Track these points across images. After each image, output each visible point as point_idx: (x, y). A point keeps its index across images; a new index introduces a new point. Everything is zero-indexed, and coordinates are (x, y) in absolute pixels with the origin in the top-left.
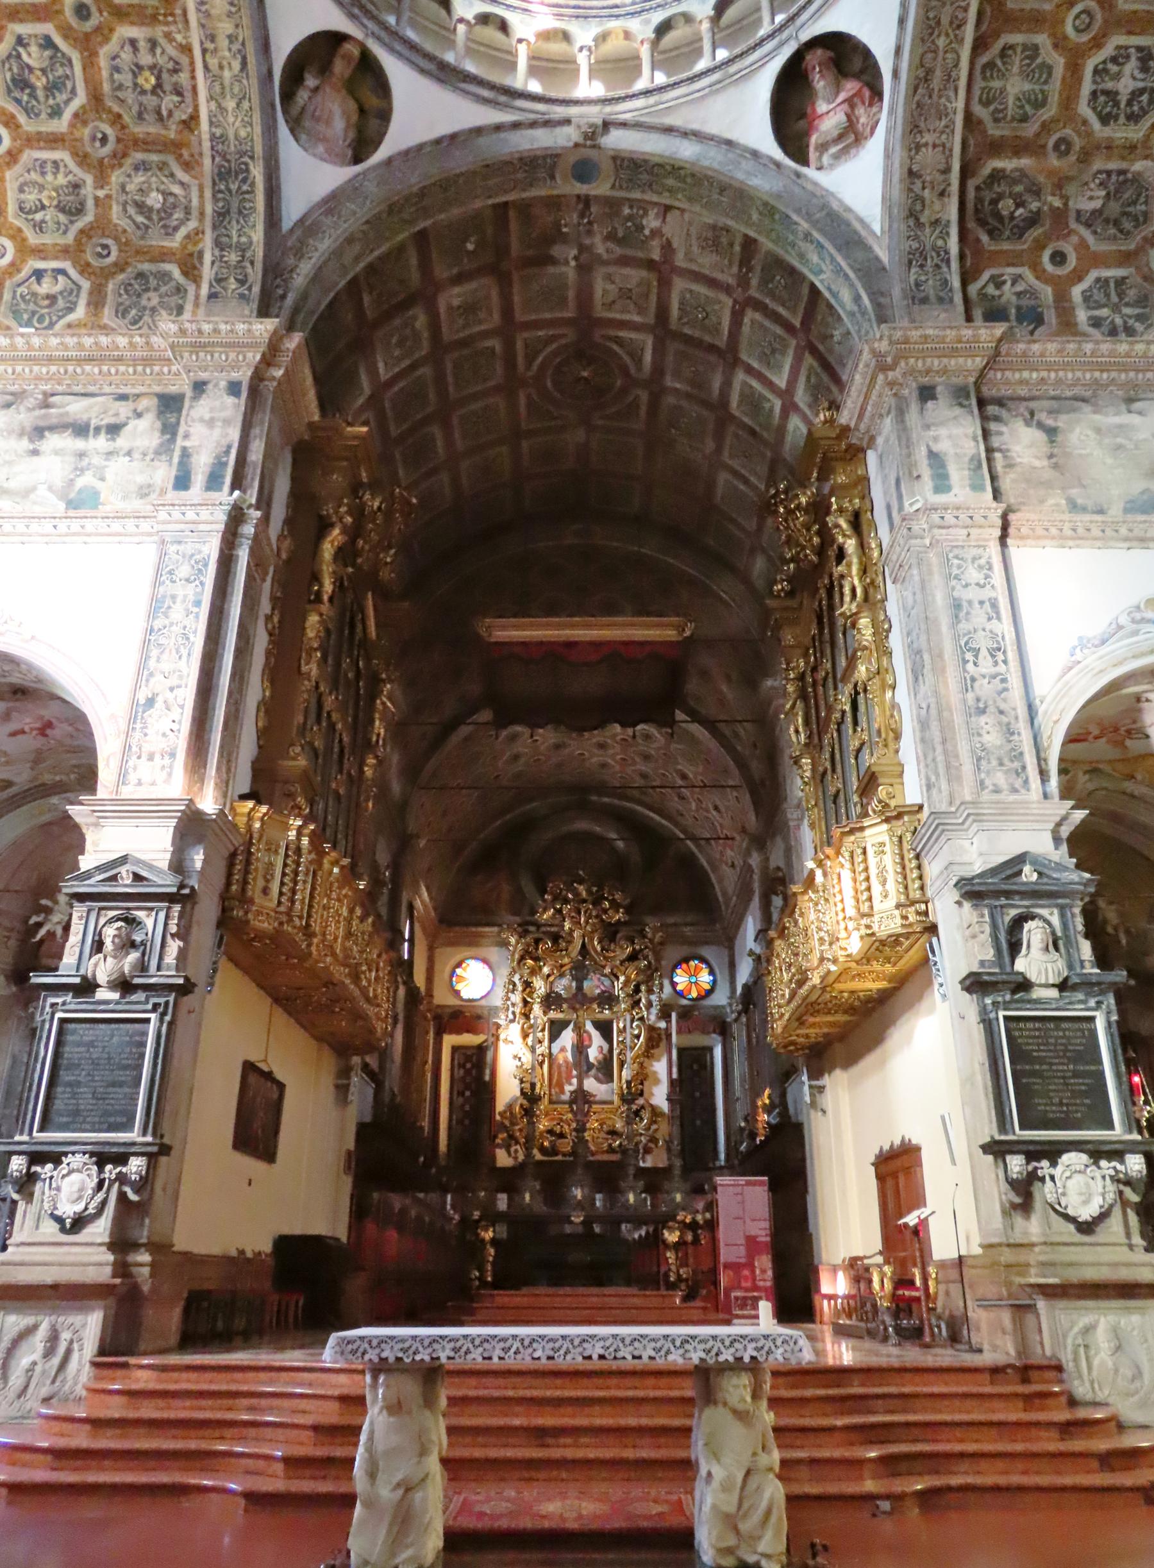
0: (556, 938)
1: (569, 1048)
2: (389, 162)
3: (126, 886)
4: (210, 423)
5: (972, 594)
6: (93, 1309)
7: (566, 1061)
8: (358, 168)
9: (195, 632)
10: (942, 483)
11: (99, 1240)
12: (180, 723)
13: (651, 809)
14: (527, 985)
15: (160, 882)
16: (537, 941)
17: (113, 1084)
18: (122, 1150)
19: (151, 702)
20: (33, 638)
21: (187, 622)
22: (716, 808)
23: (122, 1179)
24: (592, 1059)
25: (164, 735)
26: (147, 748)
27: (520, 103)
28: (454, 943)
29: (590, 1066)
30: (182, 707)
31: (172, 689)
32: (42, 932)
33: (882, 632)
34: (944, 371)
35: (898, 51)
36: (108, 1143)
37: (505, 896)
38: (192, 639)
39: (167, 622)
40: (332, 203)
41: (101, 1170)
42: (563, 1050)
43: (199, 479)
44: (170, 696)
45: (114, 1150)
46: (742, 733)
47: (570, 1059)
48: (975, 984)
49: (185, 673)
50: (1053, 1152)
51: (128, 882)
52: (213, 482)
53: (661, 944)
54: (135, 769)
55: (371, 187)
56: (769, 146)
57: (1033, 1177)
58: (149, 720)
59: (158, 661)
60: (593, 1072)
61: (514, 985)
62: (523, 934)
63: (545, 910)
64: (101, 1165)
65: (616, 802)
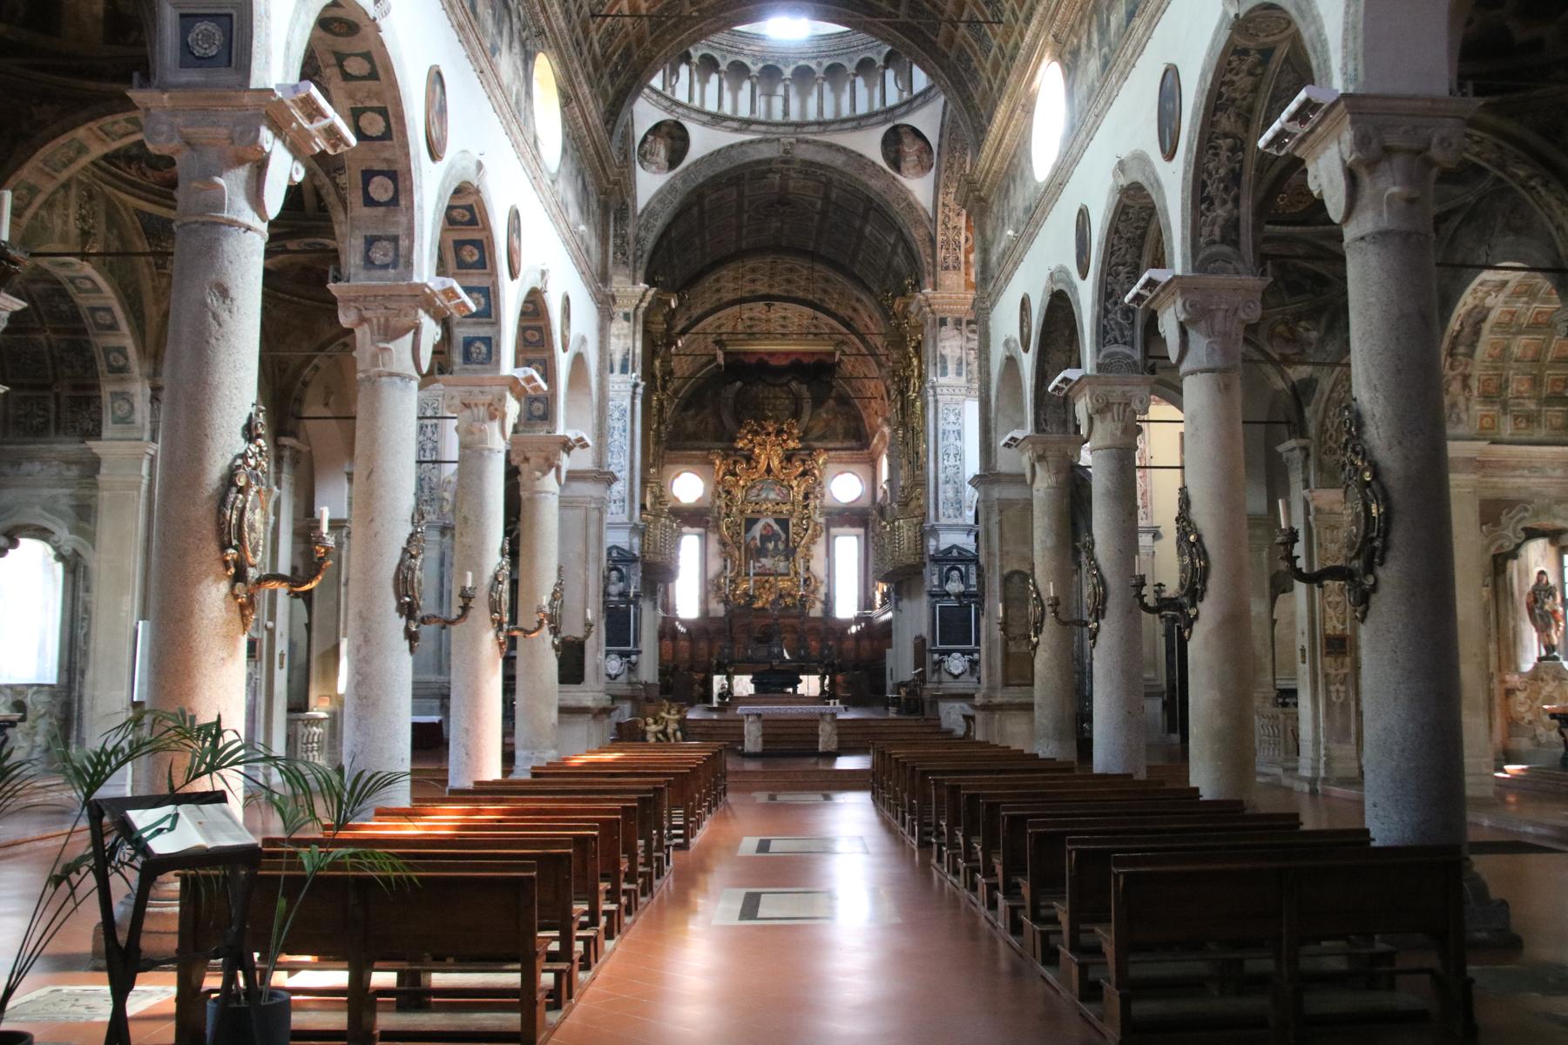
0: (748, 459)
2: (687, 168)
4: (618, 337)
5: (951, 428)
8: (672, 174)
10: (944, 374)
14: (728, 492)
16: (735, 463)
27: (754, 127)
28: (672, 463)
33: (924, 406)
34: (951, 311)
35: (941, 136)
37: (711, 427)
40: (661, 197)
42: (754, 538)
43: (617, 367)
48: (932, 595)
50: (949, 653)
52: (624, 370)
53: (825, 463)
55: (679, 184)
56: (881, 162)
57: (942, 661)
62: (726, 457)
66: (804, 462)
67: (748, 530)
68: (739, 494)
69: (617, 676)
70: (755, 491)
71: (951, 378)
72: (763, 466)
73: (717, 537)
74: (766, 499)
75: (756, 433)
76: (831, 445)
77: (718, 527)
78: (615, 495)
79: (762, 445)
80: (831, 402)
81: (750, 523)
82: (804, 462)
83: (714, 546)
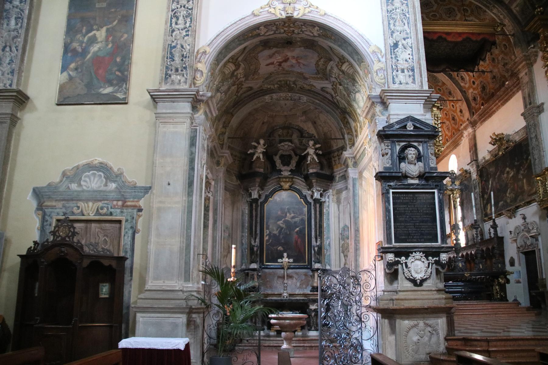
3: (411, 131)
6: (441, 317)
9: (408, 12)
11: (434, 289)
12: (412, 55)
15: (426, 129)
17: (422, 222)
18: (437, 250)
19: (396, 45)
20: (325, 14)
21: (403, 8)
23: (438, 263)
25: (406, 60)
26: (400, 67)
30: (411, 47)
31: (404, 39)
32: (255, 158)
36: (432, 247)
38: (407, 16)
39: (393, 7)
41: (428, 260)
44: (404, 42)
45: (434, 250)
46: (467, 78)
49: (408, 32)
51: (412, 129)
54: (397, 76)
58: (397, 53)
59: (394, 25)
64: (427, 257)
69: (423, 281)
78: (402, 64)
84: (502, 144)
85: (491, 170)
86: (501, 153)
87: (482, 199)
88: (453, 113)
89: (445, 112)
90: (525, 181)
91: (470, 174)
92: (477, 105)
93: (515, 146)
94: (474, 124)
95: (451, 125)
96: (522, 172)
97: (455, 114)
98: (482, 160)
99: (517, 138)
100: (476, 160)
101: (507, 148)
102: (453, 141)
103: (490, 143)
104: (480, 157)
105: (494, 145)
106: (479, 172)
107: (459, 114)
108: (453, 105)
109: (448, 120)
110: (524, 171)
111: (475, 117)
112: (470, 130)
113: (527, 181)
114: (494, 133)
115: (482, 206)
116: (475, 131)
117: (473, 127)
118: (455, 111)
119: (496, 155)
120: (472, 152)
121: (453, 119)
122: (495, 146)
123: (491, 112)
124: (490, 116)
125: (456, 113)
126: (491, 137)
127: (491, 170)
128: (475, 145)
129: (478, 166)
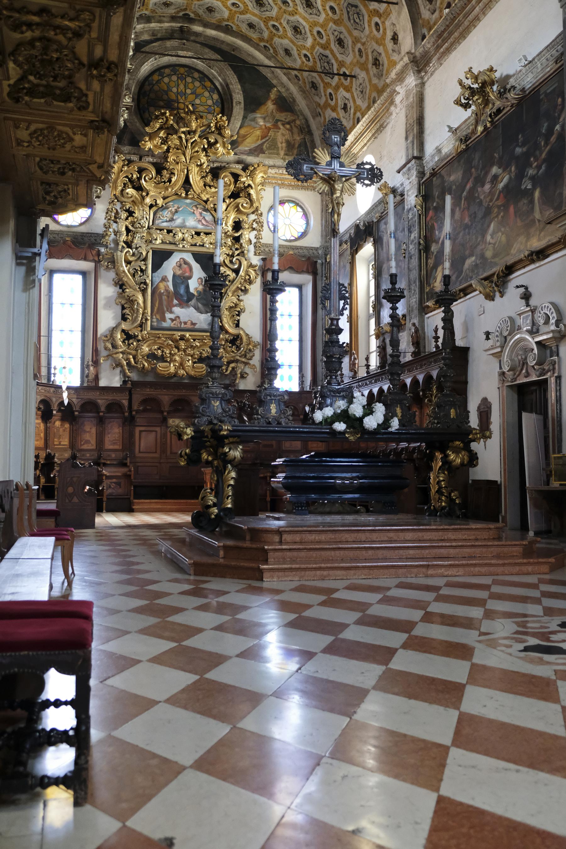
0: (159, 168)
1: (170, 278)
7: (167, 290)
13: (256, 46)
16: (141, 171)
22: (340, 42)
24: (192, 290)
29: (190, 296)
42: (164, 279)
47: (171, 288)
53: (263, 184)
60: (193, 302)
61: (117, 213)
63: (151, 137)
65: (221, 35)
66: (236, 177)
67: (156, 266)
68: (144, 216)
70: (166, 214)
71: (398, 110)
72: (178, 179)
73: (112, 275)
74: (182, 226)
75: (171, 131)
76: (271, 162)
77: (113, 262)
79: (181, 148)
80: (270, 106)
81: (160, 257)
82: (236, 177)
83: (107, 291)
84: (486, 102)
85: (452, 178)
86: (480, 129)
87: (424, 255)
88: (375, 46)
89: (359, 45)
90: (537, 194)
91: (402, 195)
92: (433, 12)
93: (520, 100)
94: (420, 64)
95: (370, 81)
96: (531, 172)
97: (381, 49)
98: (433, 156)
99: (529, 81)
100: (419, 158)
101: (499, 111)
102: (372, 121)
103: (458, 102)
104: (429, 149)
105: (466, 106)
106: (423, 188)
107: (390, 45)
108: (377, 24)
109: (363, 67)
110: (539, 167)
111: (427, 43)
112: (411, 81)
113: (542, 193)
114: (470, 69)
115: (424, 272)
116: (423, 84)
117: (419, 71)
118: (380, 42)
119: (467, 138)
120: (410, 139)
121: (376, 63)
122: (469, 111)
123: (466, 23)
124: (463, 36)
125: (384, 46)
126: (461, 83)
127: (452, 178)
128: (420, 121)
129: (421, 174)
